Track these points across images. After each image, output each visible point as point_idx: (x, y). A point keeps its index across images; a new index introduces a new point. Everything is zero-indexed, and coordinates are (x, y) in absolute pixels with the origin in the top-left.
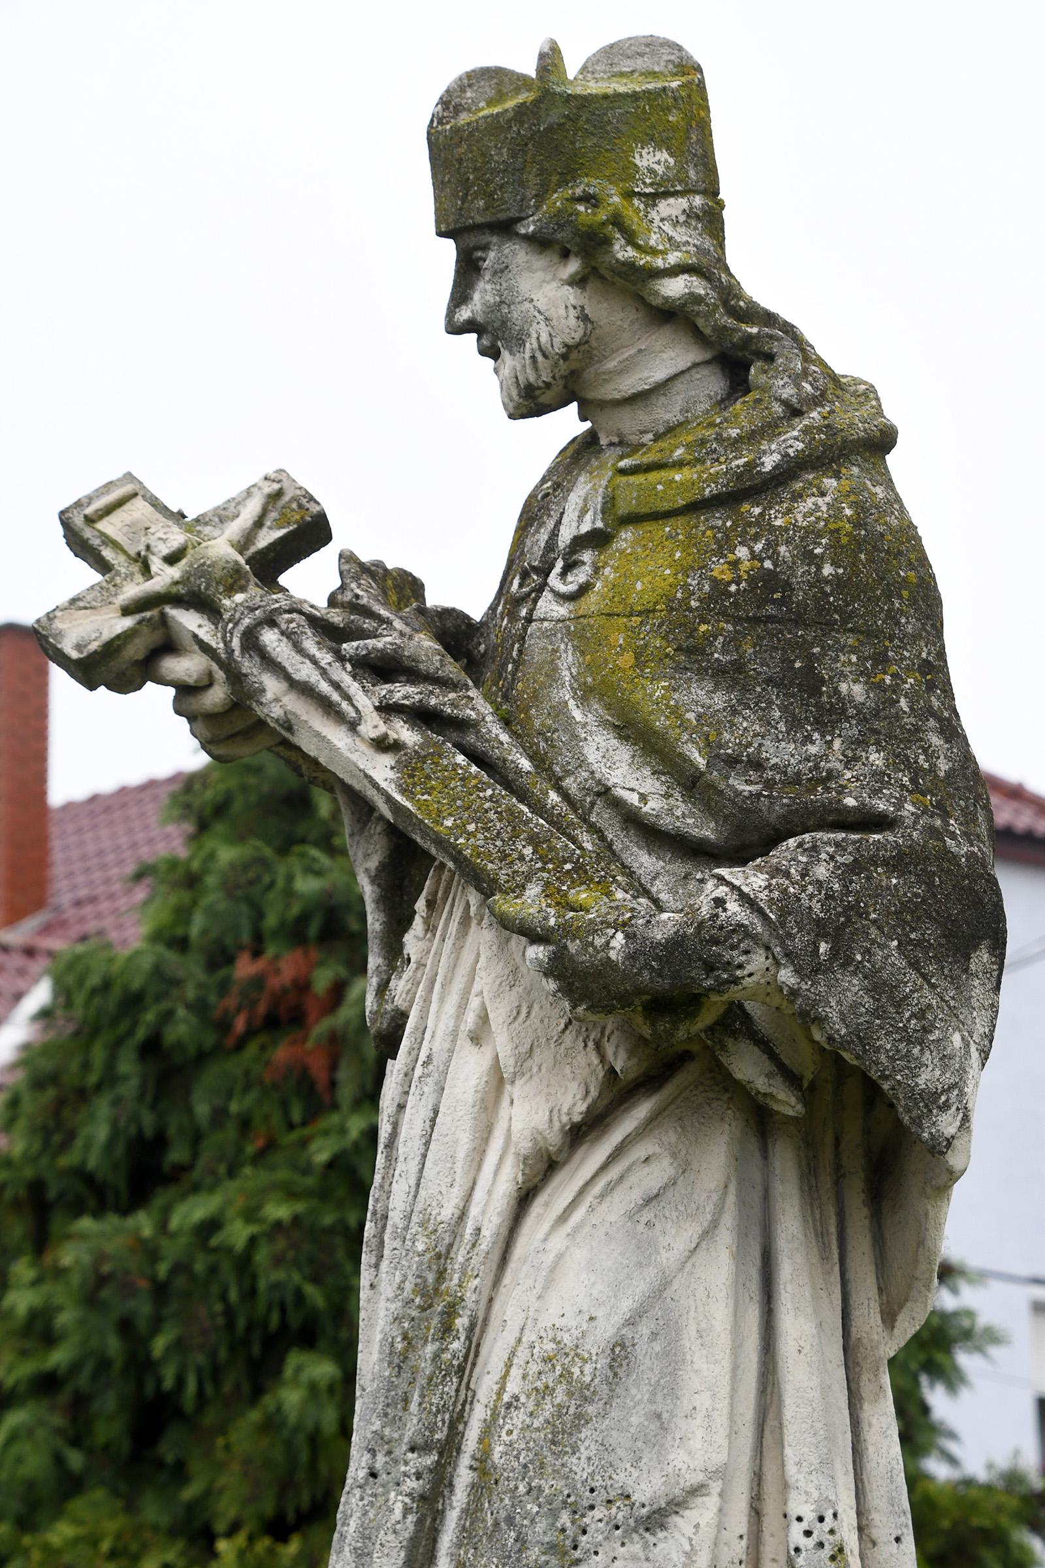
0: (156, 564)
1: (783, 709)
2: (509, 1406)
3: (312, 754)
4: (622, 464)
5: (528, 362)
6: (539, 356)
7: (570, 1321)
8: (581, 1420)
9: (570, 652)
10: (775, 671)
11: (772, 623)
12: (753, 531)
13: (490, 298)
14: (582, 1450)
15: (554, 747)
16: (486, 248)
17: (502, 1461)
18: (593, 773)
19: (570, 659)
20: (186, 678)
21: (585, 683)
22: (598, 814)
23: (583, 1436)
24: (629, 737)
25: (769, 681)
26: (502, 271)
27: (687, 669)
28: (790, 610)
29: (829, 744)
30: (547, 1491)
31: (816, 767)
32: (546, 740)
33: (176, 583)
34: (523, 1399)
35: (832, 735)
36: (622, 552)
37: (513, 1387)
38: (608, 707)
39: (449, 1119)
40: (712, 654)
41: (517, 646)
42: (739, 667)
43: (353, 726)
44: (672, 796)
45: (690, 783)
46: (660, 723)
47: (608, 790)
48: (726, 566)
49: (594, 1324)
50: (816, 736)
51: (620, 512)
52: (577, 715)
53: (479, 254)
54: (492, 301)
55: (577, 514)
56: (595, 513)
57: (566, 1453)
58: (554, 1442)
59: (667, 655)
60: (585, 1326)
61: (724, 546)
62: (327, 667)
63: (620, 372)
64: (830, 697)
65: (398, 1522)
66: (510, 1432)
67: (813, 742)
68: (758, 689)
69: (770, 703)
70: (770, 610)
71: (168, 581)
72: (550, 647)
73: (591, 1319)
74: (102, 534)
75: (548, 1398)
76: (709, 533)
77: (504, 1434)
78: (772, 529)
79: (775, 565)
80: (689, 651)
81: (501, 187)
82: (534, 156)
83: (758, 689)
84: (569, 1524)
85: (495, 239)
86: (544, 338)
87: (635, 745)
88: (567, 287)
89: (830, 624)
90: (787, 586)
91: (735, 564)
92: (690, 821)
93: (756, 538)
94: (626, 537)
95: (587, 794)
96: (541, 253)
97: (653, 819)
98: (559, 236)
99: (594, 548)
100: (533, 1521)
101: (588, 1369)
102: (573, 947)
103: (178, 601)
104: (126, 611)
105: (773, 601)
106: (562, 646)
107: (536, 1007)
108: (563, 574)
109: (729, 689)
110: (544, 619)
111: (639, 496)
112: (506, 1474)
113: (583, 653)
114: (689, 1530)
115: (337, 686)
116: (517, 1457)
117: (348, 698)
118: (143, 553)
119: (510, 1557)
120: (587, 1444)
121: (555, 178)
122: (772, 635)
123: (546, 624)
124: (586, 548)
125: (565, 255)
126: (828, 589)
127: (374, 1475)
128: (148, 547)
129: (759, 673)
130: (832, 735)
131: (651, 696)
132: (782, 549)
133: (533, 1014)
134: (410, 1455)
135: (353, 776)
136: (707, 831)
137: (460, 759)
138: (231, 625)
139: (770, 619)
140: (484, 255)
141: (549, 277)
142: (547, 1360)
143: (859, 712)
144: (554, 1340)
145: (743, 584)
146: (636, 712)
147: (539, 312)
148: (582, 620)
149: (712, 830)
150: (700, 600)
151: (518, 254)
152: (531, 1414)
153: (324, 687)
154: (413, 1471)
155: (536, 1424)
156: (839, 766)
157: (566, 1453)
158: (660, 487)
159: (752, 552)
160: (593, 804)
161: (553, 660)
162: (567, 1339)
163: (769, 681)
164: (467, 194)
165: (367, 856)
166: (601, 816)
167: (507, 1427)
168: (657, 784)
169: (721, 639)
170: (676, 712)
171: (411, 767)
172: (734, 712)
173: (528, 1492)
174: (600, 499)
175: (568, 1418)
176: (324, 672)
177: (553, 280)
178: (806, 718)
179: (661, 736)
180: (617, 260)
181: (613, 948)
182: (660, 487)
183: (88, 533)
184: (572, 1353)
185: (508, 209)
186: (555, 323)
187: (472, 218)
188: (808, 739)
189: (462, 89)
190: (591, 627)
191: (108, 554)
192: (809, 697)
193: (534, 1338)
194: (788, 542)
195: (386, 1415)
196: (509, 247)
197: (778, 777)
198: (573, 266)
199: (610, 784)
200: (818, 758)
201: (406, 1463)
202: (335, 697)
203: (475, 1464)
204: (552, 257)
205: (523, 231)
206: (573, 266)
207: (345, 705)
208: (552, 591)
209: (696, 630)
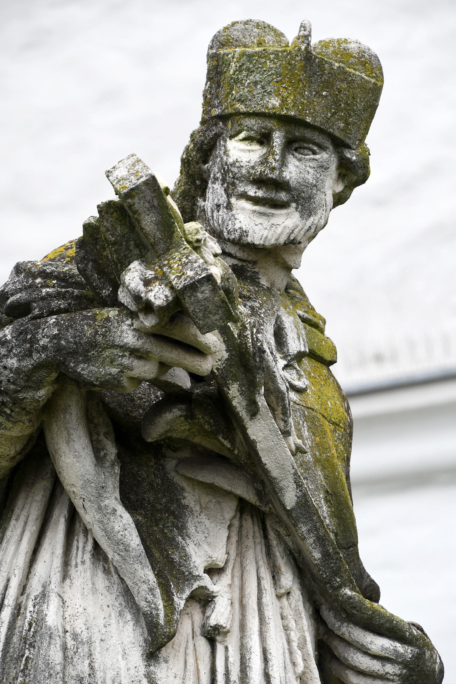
3: (252, 437)
5: (306, 228)
13: (310, 178)
16: (322, 148)
53: (315, 148)
85: (331, 148)
113: (314, 434)
190: (319, 420)
205: (348, 156)
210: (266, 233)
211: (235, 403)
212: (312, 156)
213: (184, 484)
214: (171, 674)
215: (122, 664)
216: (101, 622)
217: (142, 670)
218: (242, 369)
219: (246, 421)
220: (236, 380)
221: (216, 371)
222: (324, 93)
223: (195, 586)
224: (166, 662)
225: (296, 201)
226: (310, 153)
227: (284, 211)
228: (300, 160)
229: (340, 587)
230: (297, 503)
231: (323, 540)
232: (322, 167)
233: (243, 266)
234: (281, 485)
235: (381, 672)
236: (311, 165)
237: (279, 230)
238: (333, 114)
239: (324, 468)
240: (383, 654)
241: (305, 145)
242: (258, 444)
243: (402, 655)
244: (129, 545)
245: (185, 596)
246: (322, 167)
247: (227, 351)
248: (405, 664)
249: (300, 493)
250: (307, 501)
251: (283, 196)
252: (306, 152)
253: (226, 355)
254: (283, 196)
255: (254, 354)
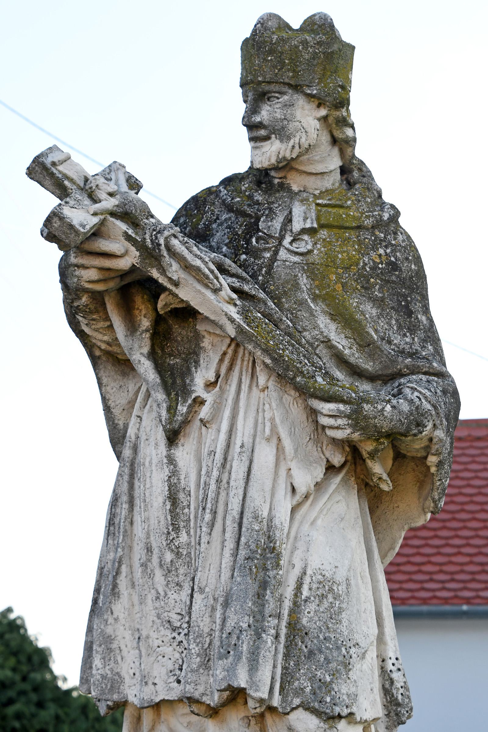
0: (102, 195)
1: (397, 320)
2: (306, 601)
4: (320, 201)
6: (297, 147)
7: (327, 567)
8: (341, 610)
9: (305, 278)
10: (395, 305)
11: (393, 284)
12: (384, 244)
13: (278, 115)
14: (343, 622)
15: (298, 317)
17: (308, 624)
18: (322, 332)
19: (305, 281)
20: (116, 251)
21: (315, 293)
22: (320, 350)
23: (343, 616)
24: (337, 320)
25: (393, 308)
26: (290, 106)
27: (364, 296)
28: (400, 280)
29: (413, 339)
30: (333, 639)
31: (411, 347)
32: (292, 314)
33: (117, 206)
34: (312, 598)
35: (414, 335)
36: (324, 240)
37: (305, 592)
38: (328, 305)
39: (259, 473)
40: (374, 292)
41: (264, 269)
42: (382, 299)
43: (216, 291)
44: (352, 348)
45: (365, 344)
46: (358, 316)
47: (329, 340)
48: (377, 256)
49: (337, 570)
50: (408, 334)
51: (322, 222)
52: (312, 305)
53: (277, 95)
54: (279, 117)
55: (302, 218)
56: (312, 220)
57: (337, 623)
58: (331, 618)
59: (357, 289)
60: (334, 570)
61: (374, 248)
62: (208, 261)
63: (318, 162)
64: (415, 319)
65: (270, 647)
66: (309, 613)
67: (407, 337)
68: (388, 310)
69: (392, 317)
70: (394, 278)
71: (113, 204)
72: (293, 274)
73: (336, 567)
74: (60, 172)
75: (325, 600)
76: (367, 240)
77: (306, 613)
78: (392, 245)
79: (396, 260)
80: (366, 289)
81: (303, 70)
82: (323, 62)
83: (388, 310)
84: (346, 654)
85: (290, 91)
86: (303, 140)
87: (339, 324)
88: (316, 120)
89: (414, 289)
90: (401, 270)
91: (380, 255)
92: (361, 361)
93: (386, 247)
94: (324, 234)
95: (317, 341)
96: (309, 103)
97: (348, 357)
98: (327, 99)
99: (309, 235)
100: (331, 651)
101: (340, 588)
102: (366, 407)
103: (113, 214)
104: (95, 214)
105: (395, 275)
106: (300, 275)
107: (297, 429)
108: (291, 243)
109: (378, 308)
110: (286, 261)
111: (334, 217)
112: (312, 630)
113: (313, 280)
114: (370, 661)
115: (212, 272)
116: (315, 623)
117: (217, 278)
118: (94, 188)
119: (323, 666)
120: (345, 620)
121: (329, 73)
122: (393, 289)
123: (287, 263)
124: (305, 233)
125: (319, 106)
126: (413, 275)
127: (249, 626)
128: (97, 186)
129: (389, 304)
130: (414, 335)
131: (352, 304)
132: (398, 254)
133: (296, 432)
134: (270, 619)
135: (215, 312)
136: (369, 366)
137: (259, 315)
138: (155, 233)
139: (393, 282)
140: (279, 96)
141: (310, 114)
142: (320, 583)
143: (424, 328)
144: (321, 574)
145: (384, 265)
146: (346, 310)
147: (303, 128)
148: (310, 265)
149: (370, 366)
150: (370, 268)
151: (301, 101)
152: (318, 605)
153: (207, 271)
154: (273, 625)
155: (321, 610)
156: (419, 349)
157: (337, 623)
158: (344, 216)
159: (386, 253)
160: (318, 346)
161: (296, 280)
162: (327, 575)
163: (393, 308)
164: (283, 68)
165: (140, 347)
166: (322, 350)
167: (307, 610)
168: (347, 342)
169: (378, 286)
170: (363, 313)
171: (244, 313)
172: (379, 318)
173: (325, 639)
174: (313, 214)
175: (336, 609)
176: (206, 263)
177: (311, 116)
178: (405, 326)
179: (359, 322)
180: (342, 115)
181: (386, 411)
182: (344, 216)
183: (55, 171)
184: (332, 581)
185: (305, 80)
186: (309, 134)
187: (283, 79)
188: (405, 335)
189: (268, 20)
190: (318, 269)
191: (66, 183)
192: (407, 318)
193: (311, 573)
194: (400, 251)
195: (252, 600)
196: (296, 96)
197: (396, 349)
198: (323, 112)
199: (331, 339)
200: (411, 344)
201: (268, 622)
202: (211, 276)
203: (287, 625)
204: (314, 106)
205: (309, 92)
206: (323, 112)
207: (215, 280)
208: (286, 249)
209: (369, 280)
210: (260, 159)
211: (160, 281)
212: (277, 101)
213: (205, 333)
214: (185, 452)
215: (154, 452)
216: (148, 429)
217: (165, 453)
218: (153, 259)
219: (174, 290)
220: (152, 267)
221: (136, 265)
222: (269, 58)
223: (193, 397)
224: (183, 445)
225: (274, 133)
226: (275, 99)
227: (268, 142)
228: (270, 106)
229: (294, 377)
230: (237, 332)
231: (268, 351)
232: (286, 105)
233: (282, 182)
234: (220, 323)
235: (336, 425)
236: (277, 106)
237: (268, 154)
238: (279, 70)
239: (324, 300)
240: (331, 413)
241: (270, 95)
242: (190, 302)
243: (343, 412)
244: (148, 381)
245: (187, 404)
246: (286, 105)
247: (137, 251)
248: (349, 417)
249: (235, 326)
250: (242, 330)
251: (263, 132)
252: (272, 99)
253: (138, 254)
254: (263, 132)
255: (154, 248)
